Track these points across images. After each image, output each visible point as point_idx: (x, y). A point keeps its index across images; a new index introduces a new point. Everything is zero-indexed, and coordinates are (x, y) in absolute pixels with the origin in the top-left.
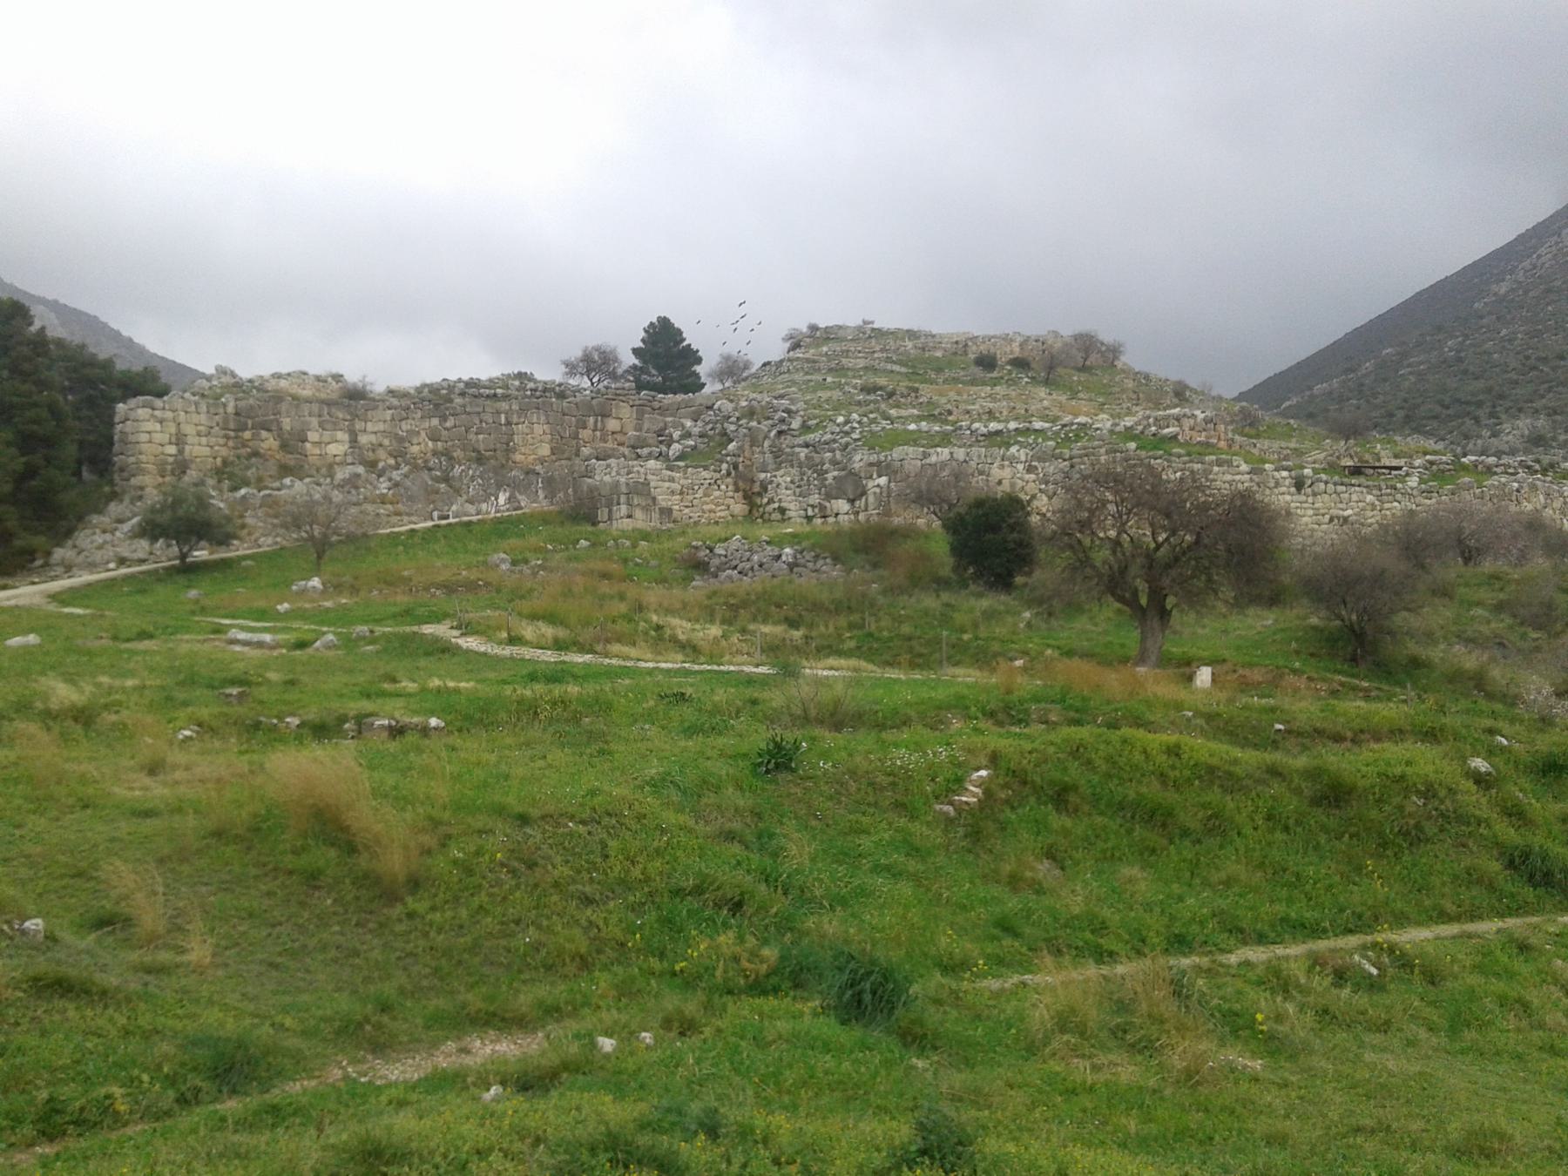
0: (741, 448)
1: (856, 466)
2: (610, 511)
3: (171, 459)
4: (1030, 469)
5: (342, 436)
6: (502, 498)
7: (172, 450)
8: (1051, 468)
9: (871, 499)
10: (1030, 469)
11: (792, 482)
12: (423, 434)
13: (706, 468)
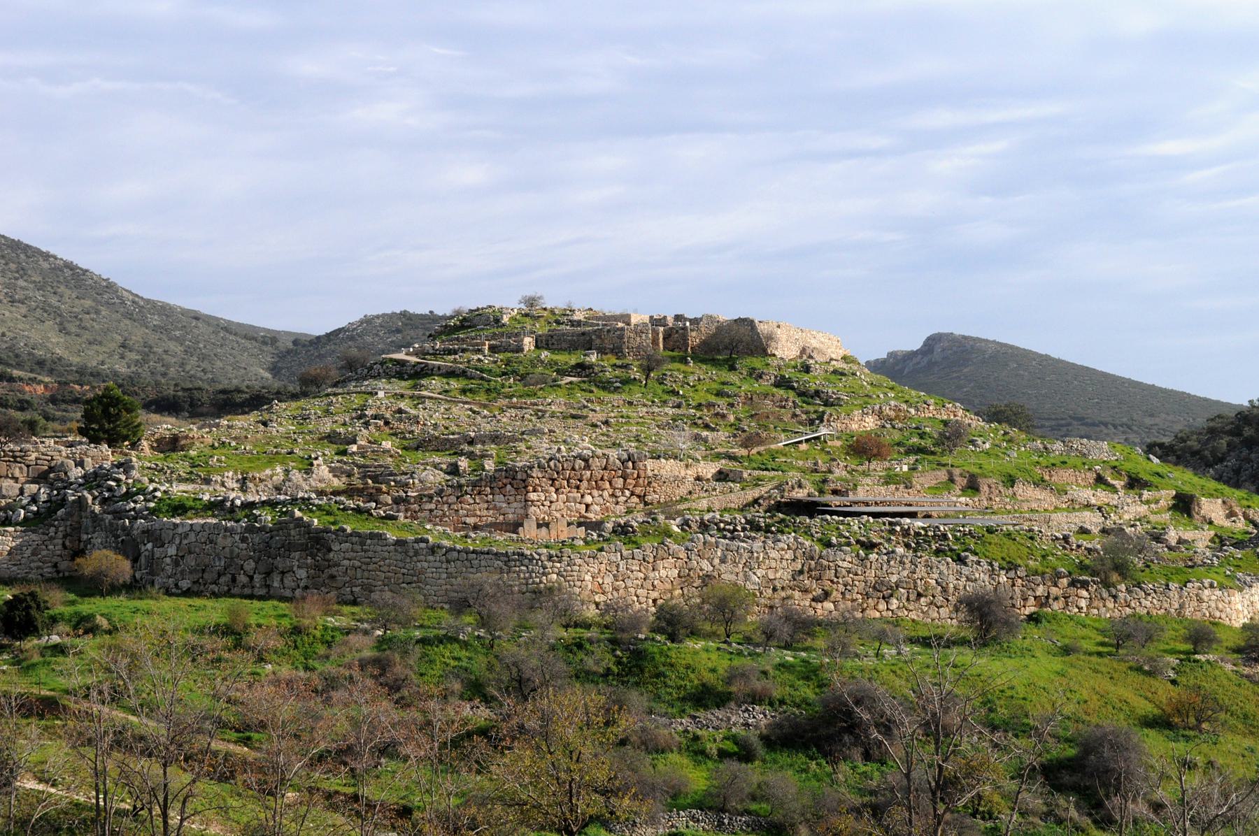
0: (69, 514)
4: (243, 540)
8: (257, 538)
10: (243, 540)
13: (34, 532)
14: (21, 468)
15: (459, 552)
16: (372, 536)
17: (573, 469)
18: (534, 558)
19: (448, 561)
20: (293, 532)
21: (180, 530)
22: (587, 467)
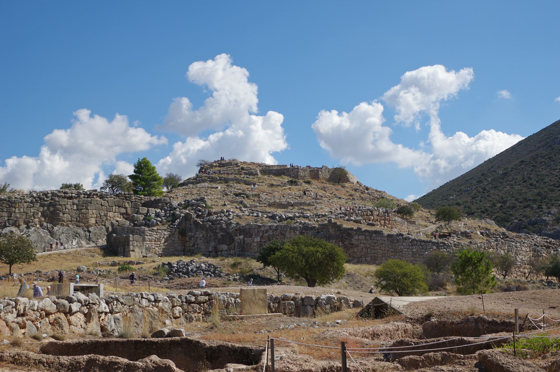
1: (230, 231)
2: (124, 249)
5: (5, 214)
6: (74, 243)
9: (236, 244)
11: (203, 237)
12: (40, 214)
14: (128, 203)
15: (417, 241)
16: (376, 232)
17: (367, 215)
18: (449, 246)
19: (412, 246)
20: (331, 230)
21: (263, 229)
22: (372, 215)
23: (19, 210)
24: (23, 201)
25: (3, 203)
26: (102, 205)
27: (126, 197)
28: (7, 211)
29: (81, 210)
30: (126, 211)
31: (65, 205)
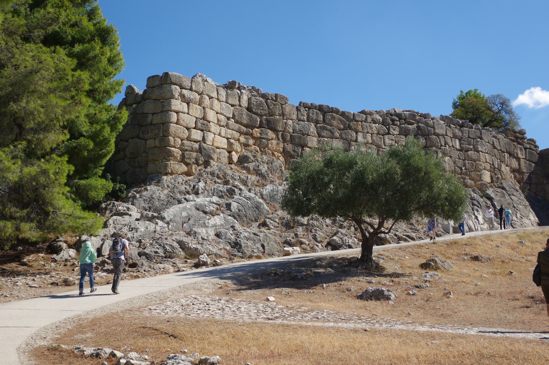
3: (196, 146)
7: (197, 135)
14: (521, 149)
23: (365, 137)
24: (369, 119)
25: (333, 118)
26: (494, 147)
27: (517, 138)
28: (341, 138)
29: (467, 151)
30: (519, 164)
31: (443, 135)
